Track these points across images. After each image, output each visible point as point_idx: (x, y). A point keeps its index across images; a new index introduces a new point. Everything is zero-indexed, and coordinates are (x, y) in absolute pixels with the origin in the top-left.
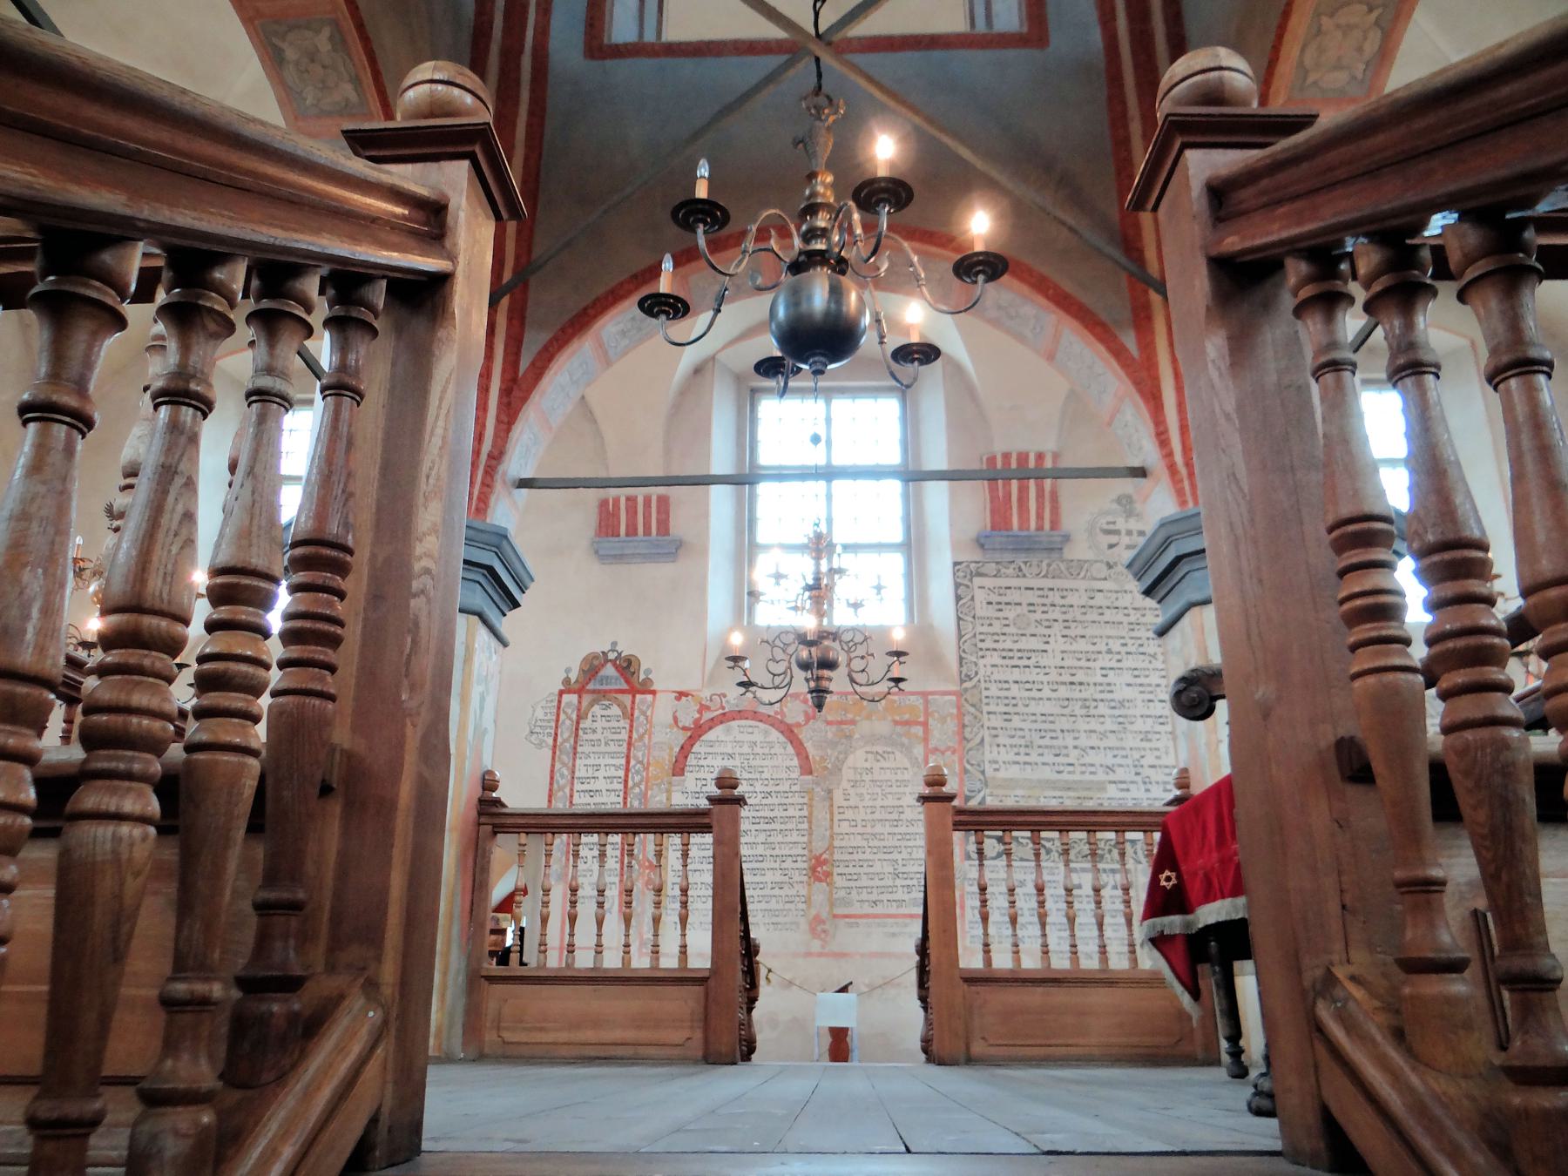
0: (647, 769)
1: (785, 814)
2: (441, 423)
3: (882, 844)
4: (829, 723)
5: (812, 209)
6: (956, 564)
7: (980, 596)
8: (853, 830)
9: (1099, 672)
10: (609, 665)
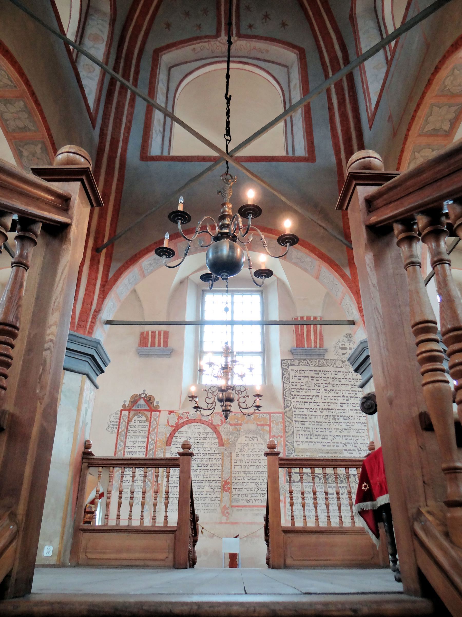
0: (156, 443)
1: (212, 463)
2: (61, 282)
3: (252, 475)
4: (230, 425)
5: (223, 217)
6: (282, 360)
7: (292, 374)
8: (240, 470)
9: (339, 405)
10: (142, 399)
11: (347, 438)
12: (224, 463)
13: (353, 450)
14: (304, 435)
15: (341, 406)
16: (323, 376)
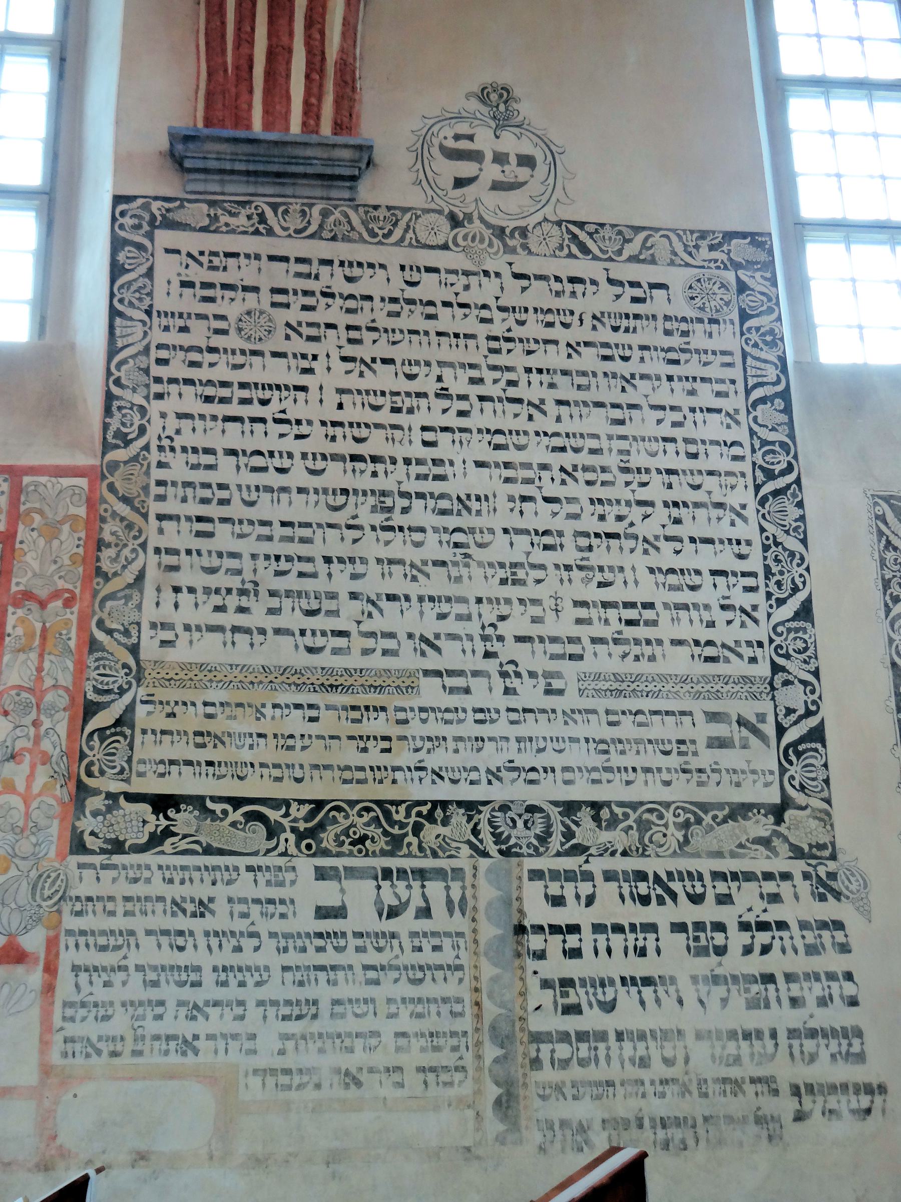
6: (118, 199)
7: (167, 269)
11: (445, 608)
13: (476, 674)
14: (207, 591)
15: (426, 444)
16: (340, 286)
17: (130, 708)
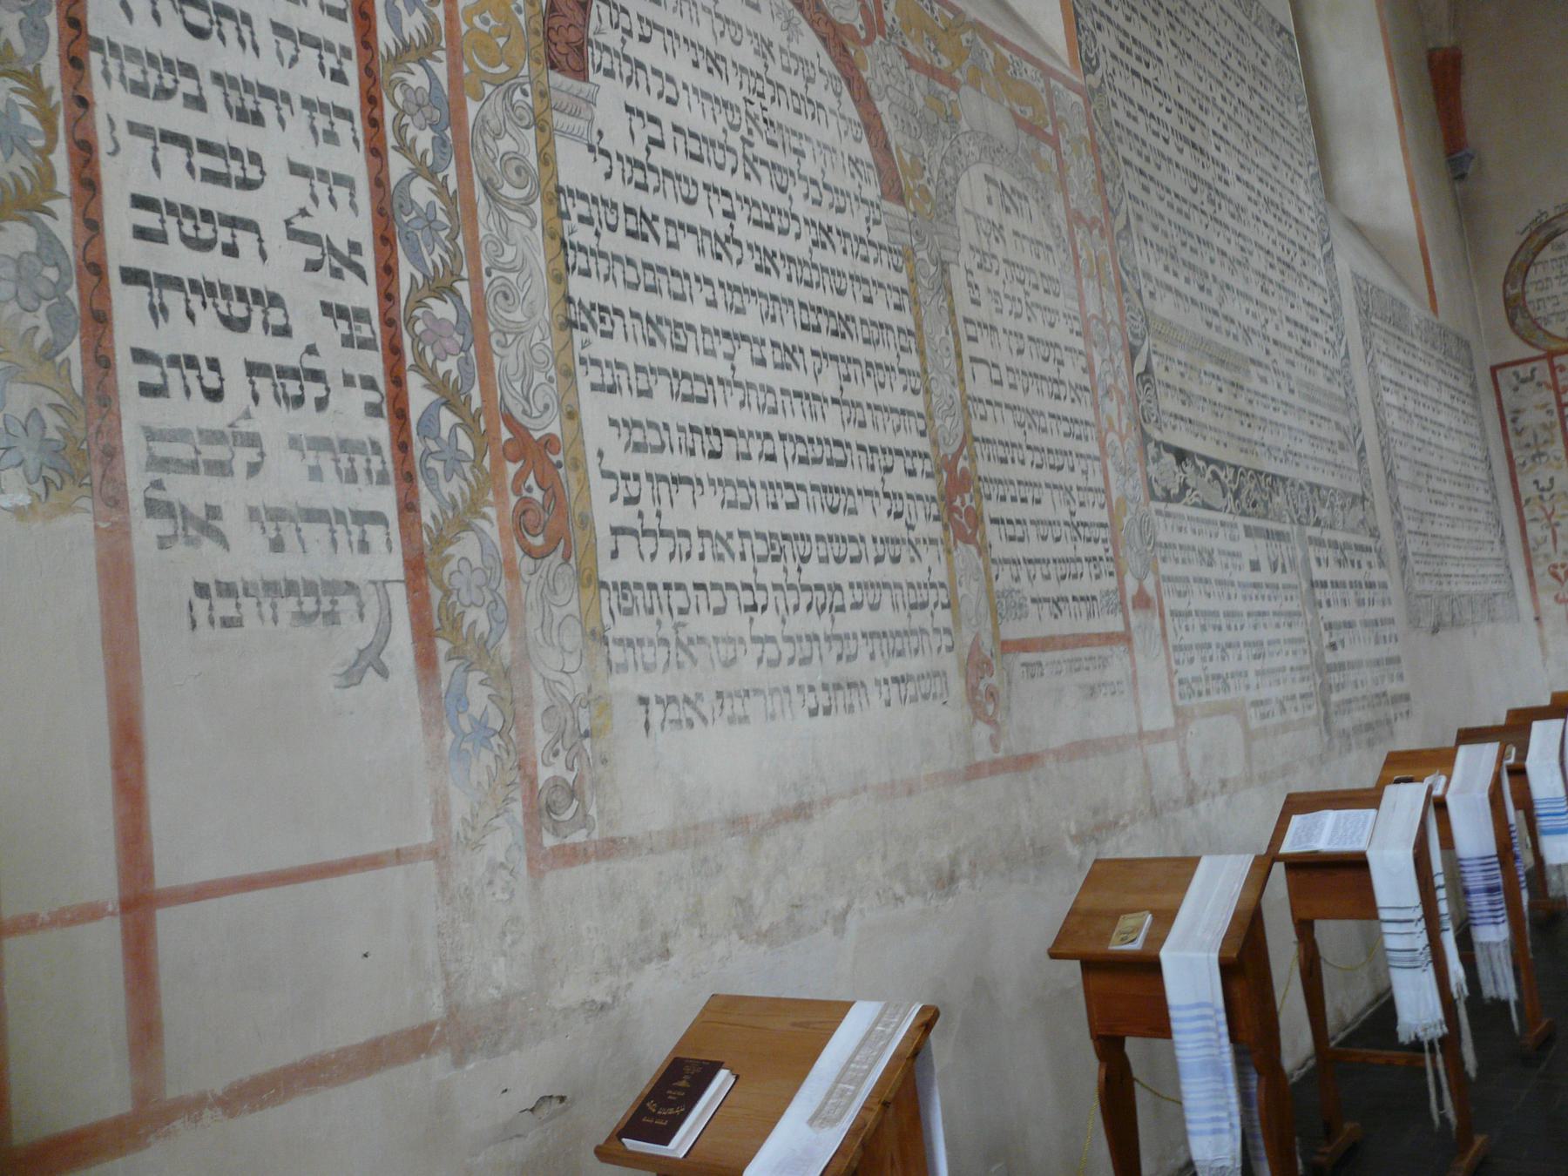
12: (927, 328)
17: (1149, 359)
